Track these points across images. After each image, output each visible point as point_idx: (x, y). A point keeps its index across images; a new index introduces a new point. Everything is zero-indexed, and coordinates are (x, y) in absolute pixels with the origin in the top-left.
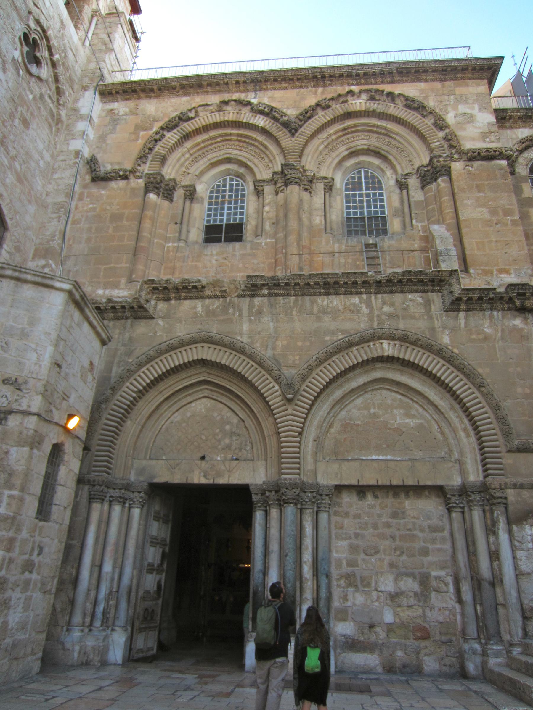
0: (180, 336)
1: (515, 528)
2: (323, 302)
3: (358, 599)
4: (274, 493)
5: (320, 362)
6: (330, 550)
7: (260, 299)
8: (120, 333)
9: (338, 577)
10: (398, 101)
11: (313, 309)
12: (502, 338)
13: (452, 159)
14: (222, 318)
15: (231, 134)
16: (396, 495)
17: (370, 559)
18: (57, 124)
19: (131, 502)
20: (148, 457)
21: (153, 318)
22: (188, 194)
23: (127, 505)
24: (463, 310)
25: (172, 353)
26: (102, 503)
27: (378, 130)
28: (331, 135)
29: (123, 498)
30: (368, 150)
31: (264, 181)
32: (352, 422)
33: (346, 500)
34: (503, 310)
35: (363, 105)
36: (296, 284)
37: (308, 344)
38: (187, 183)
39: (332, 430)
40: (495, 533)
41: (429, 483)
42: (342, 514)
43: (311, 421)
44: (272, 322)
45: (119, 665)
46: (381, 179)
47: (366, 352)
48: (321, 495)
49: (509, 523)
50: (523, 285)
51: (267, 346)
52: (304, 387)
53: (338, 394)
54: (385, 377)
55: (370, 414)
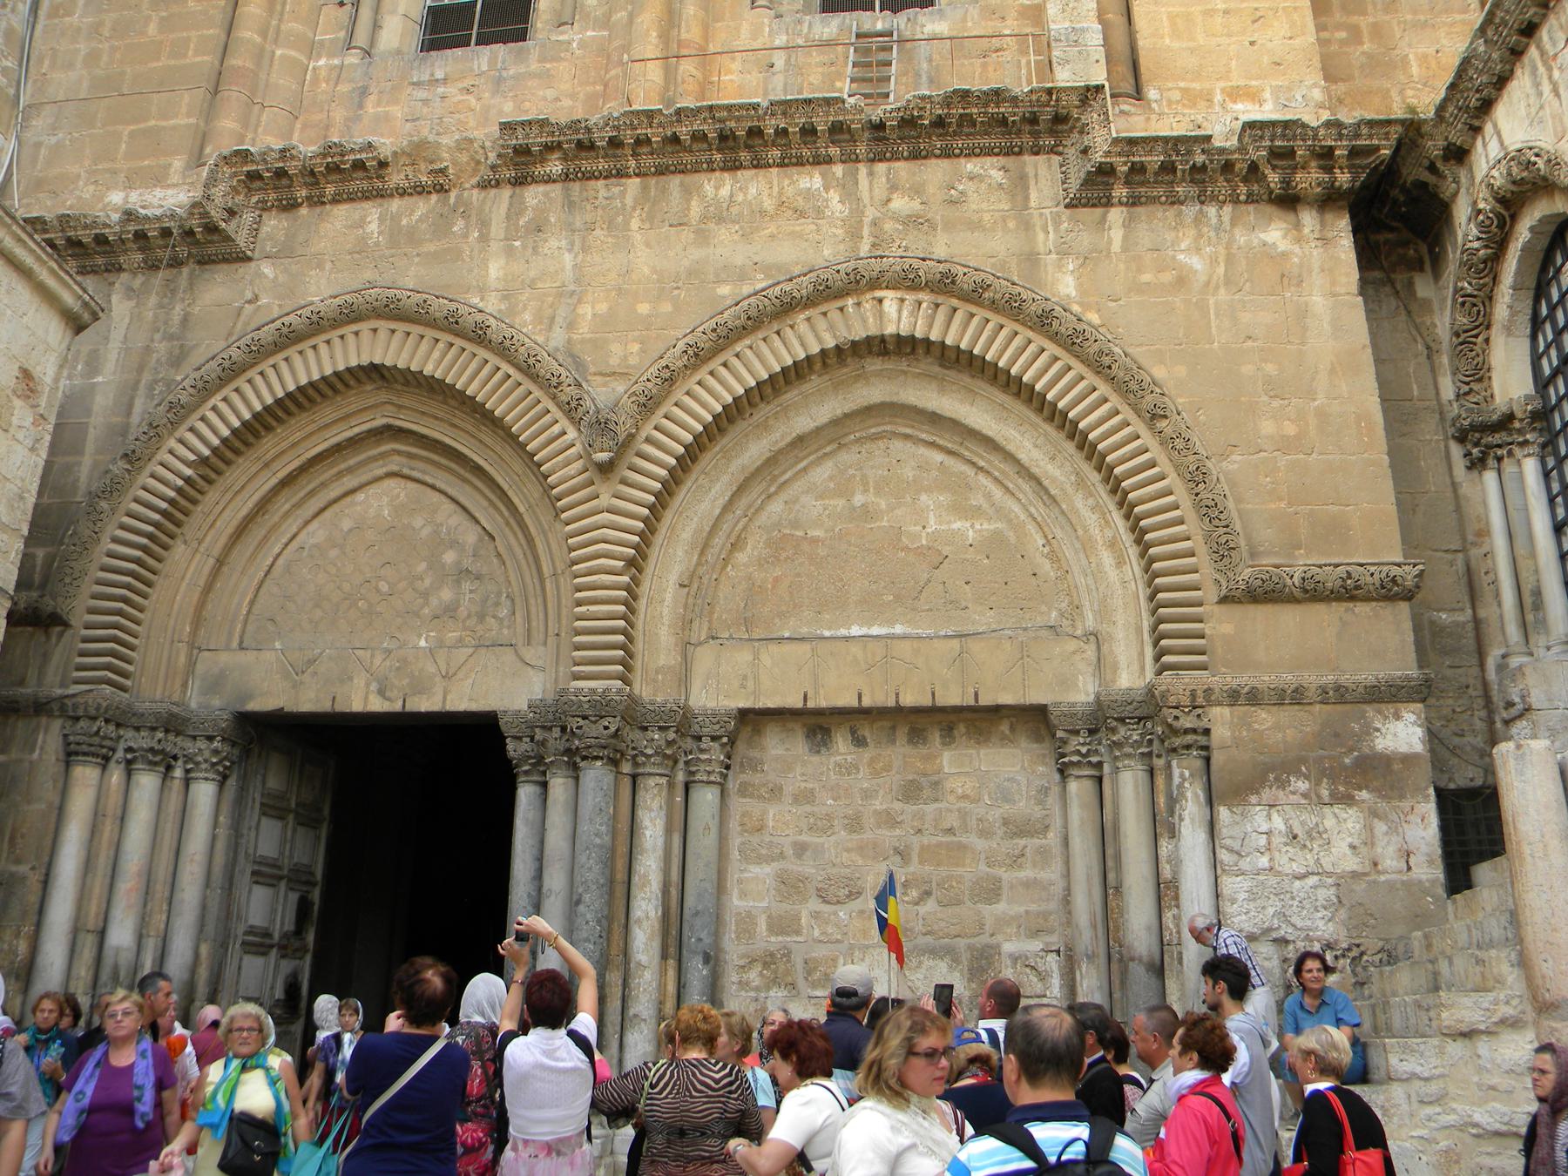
0: (312, 303)
2: (717, 188)
4: (556, 732)
5: (698, 357)
6: (720, 888)
7: (541, 188)
8: (161, 306)
9: (742, 963)
11: (689, 209)
12: (1228, 281)
14: (431, 247)
16: (917, 735)
17: (835, 913)
19: (190, 766)
20: (235, 644)
21: (250, 259)
23: (178, 773)
24: (1121, 203)
25: (291, 352)
26: (104, 768)
29: (162, 752)
32: (800, 533)
33: (773, 752)
34: (1236, 201)
36: (639, 142)
37: (667, 307)
39: (741, 557)
40: (1173, 833)
41: (1007, 699)
42: (763, 790)
43: (672, 528)
44: (570, 251)
47: (832, 328)
48: (699, 738)
49: (1210, 802)
50: (1286, 124)
51: (552, 319)
52: (648, 430)
53: (753, 449)
54: (895, 399)
55: (854, 509)
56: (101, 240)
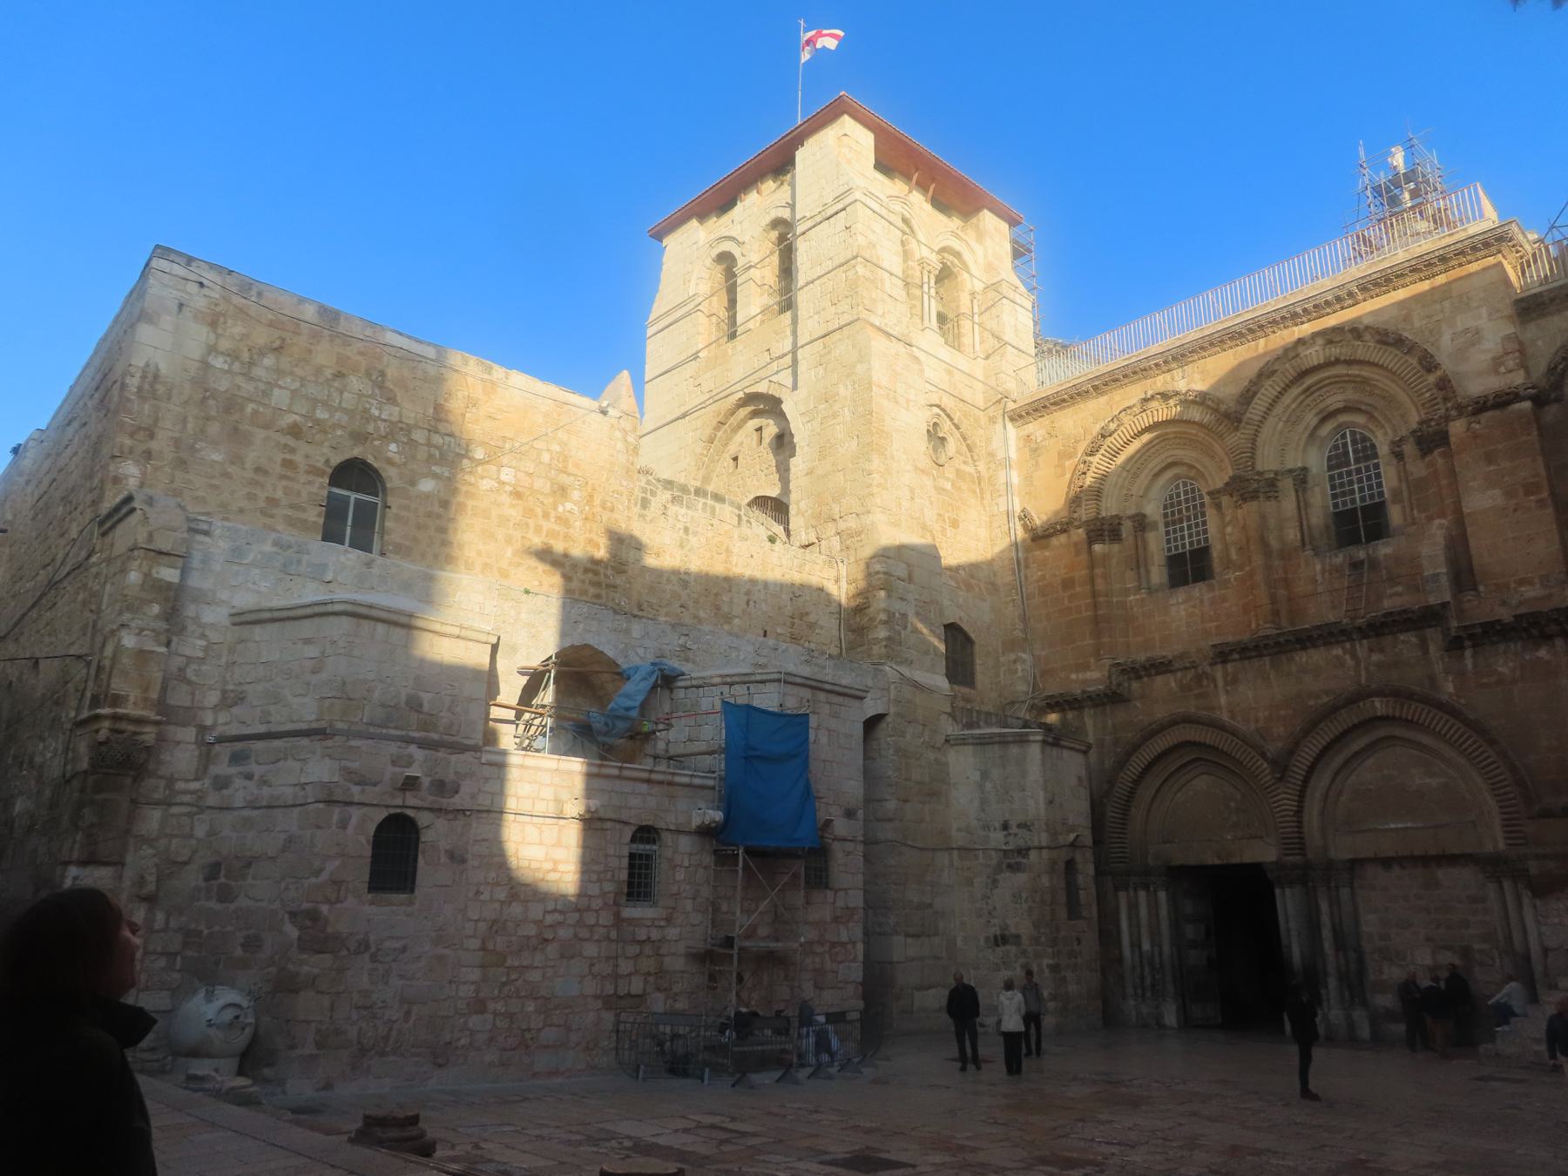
1: (1538, 903)
5: (1307, 732)
7: (1233, 664)
10: (1367, 337)
13: (1447, 419)
14: (1196, 692)
15: (1167, 434)
18: (979, 484)
21: (1129, 701)
22: (1136, 525)
23: (1152, 889)
27: (1351, 379)
28: (1288, 406)
30: (1345, 407)
31: (1218, 491)
35: (1321, 352)
38: (1132, 511)
41: (1456, 852)
46: (1374, 441)
53: (1339, 760)
56: (1076, 699)
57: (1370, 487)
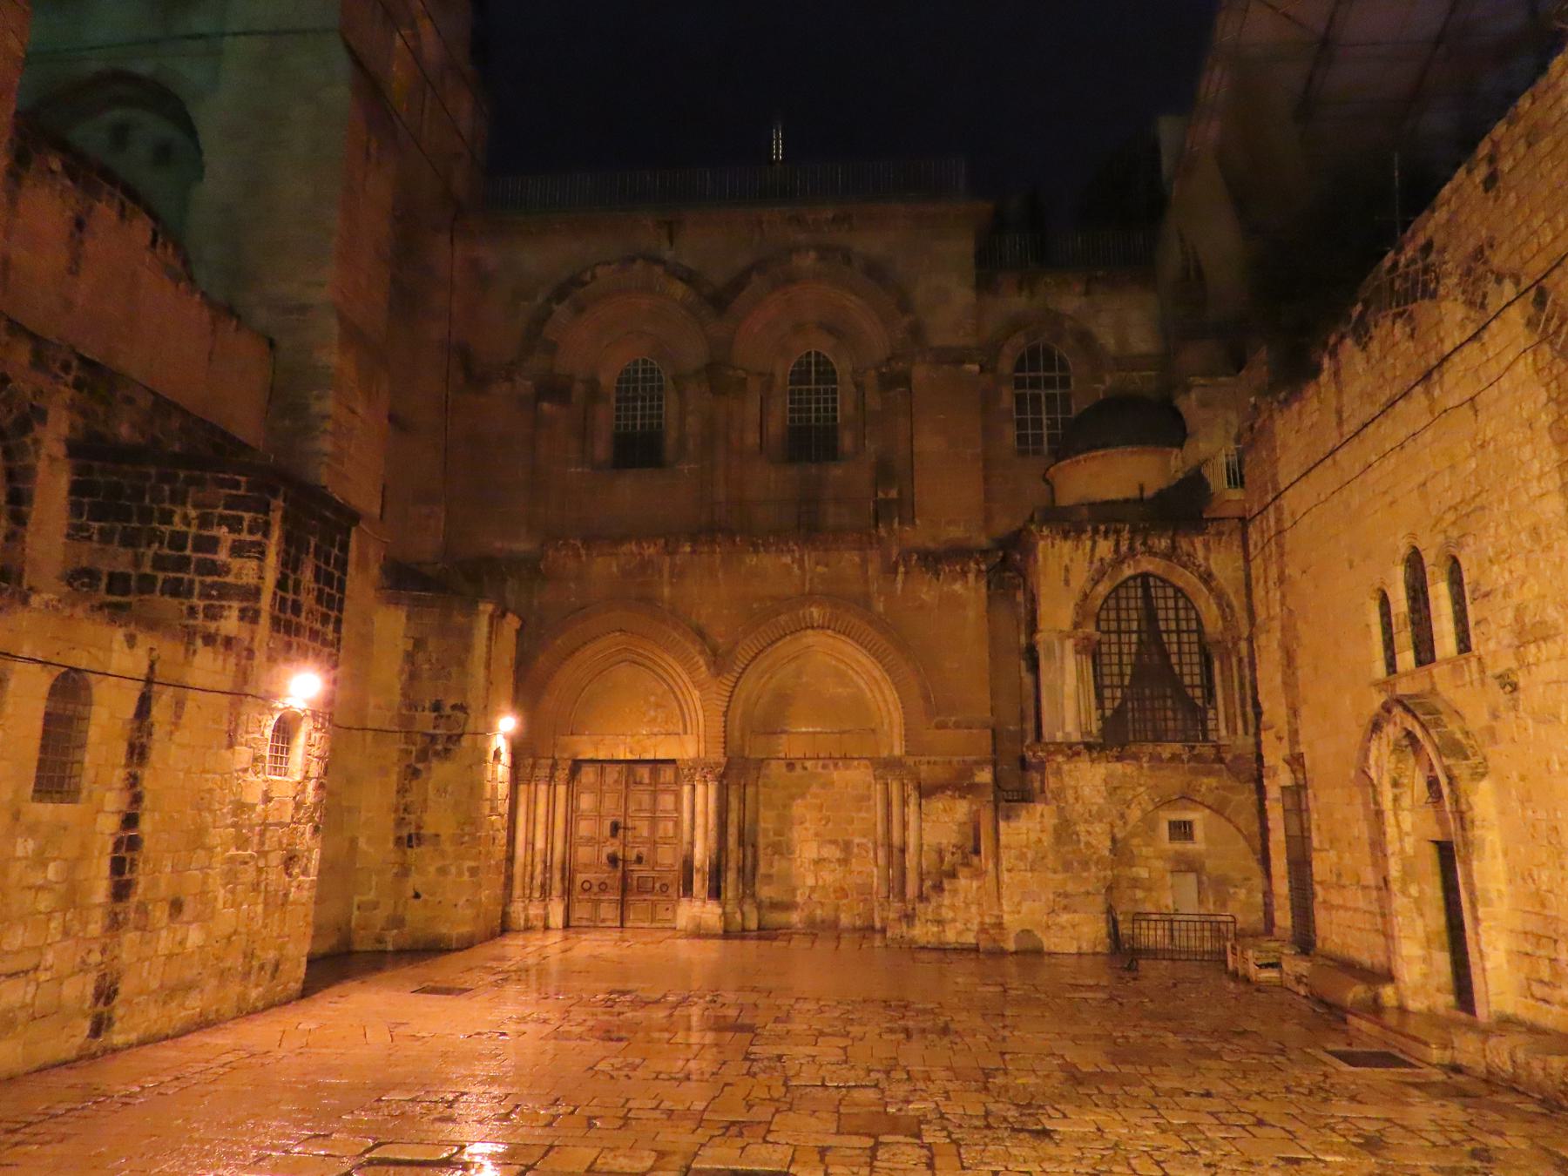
3: (784, 864)
45: (558, 929)
46: (836, 366)
49: (920, 797)
57: (826, 409)
